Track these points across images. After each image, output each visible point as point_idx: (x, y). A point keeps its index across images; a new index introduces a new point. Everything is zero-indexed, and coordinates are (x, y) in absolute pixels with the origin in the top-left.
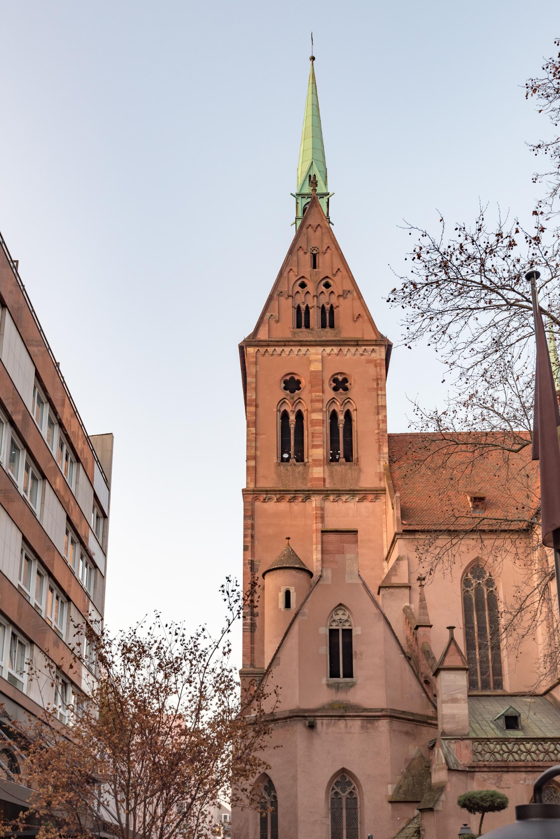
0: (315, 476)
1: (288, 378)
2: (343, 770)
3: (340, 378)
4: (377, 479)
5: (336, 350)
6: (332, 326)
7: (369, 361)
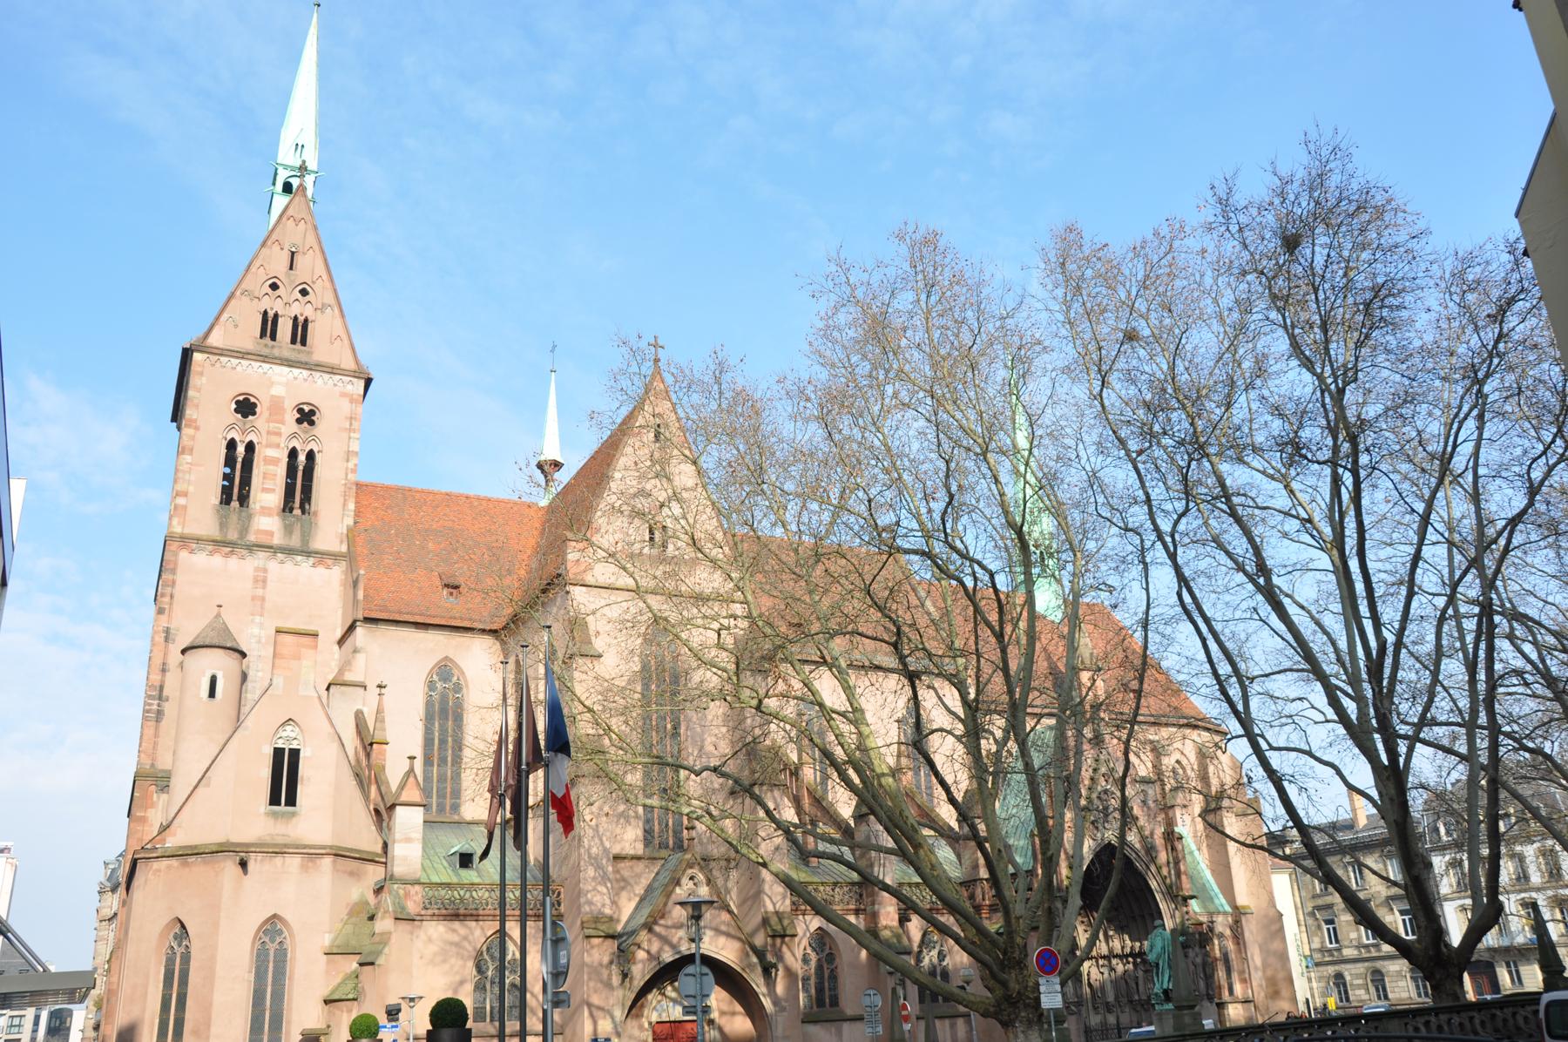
0: (262, 527)
1: (241, 398)
2: (275, 916)
3: (307, 409)
4: (338, 541)
5: (305, 373)
6: (304, 343)
7: (343, 395)
